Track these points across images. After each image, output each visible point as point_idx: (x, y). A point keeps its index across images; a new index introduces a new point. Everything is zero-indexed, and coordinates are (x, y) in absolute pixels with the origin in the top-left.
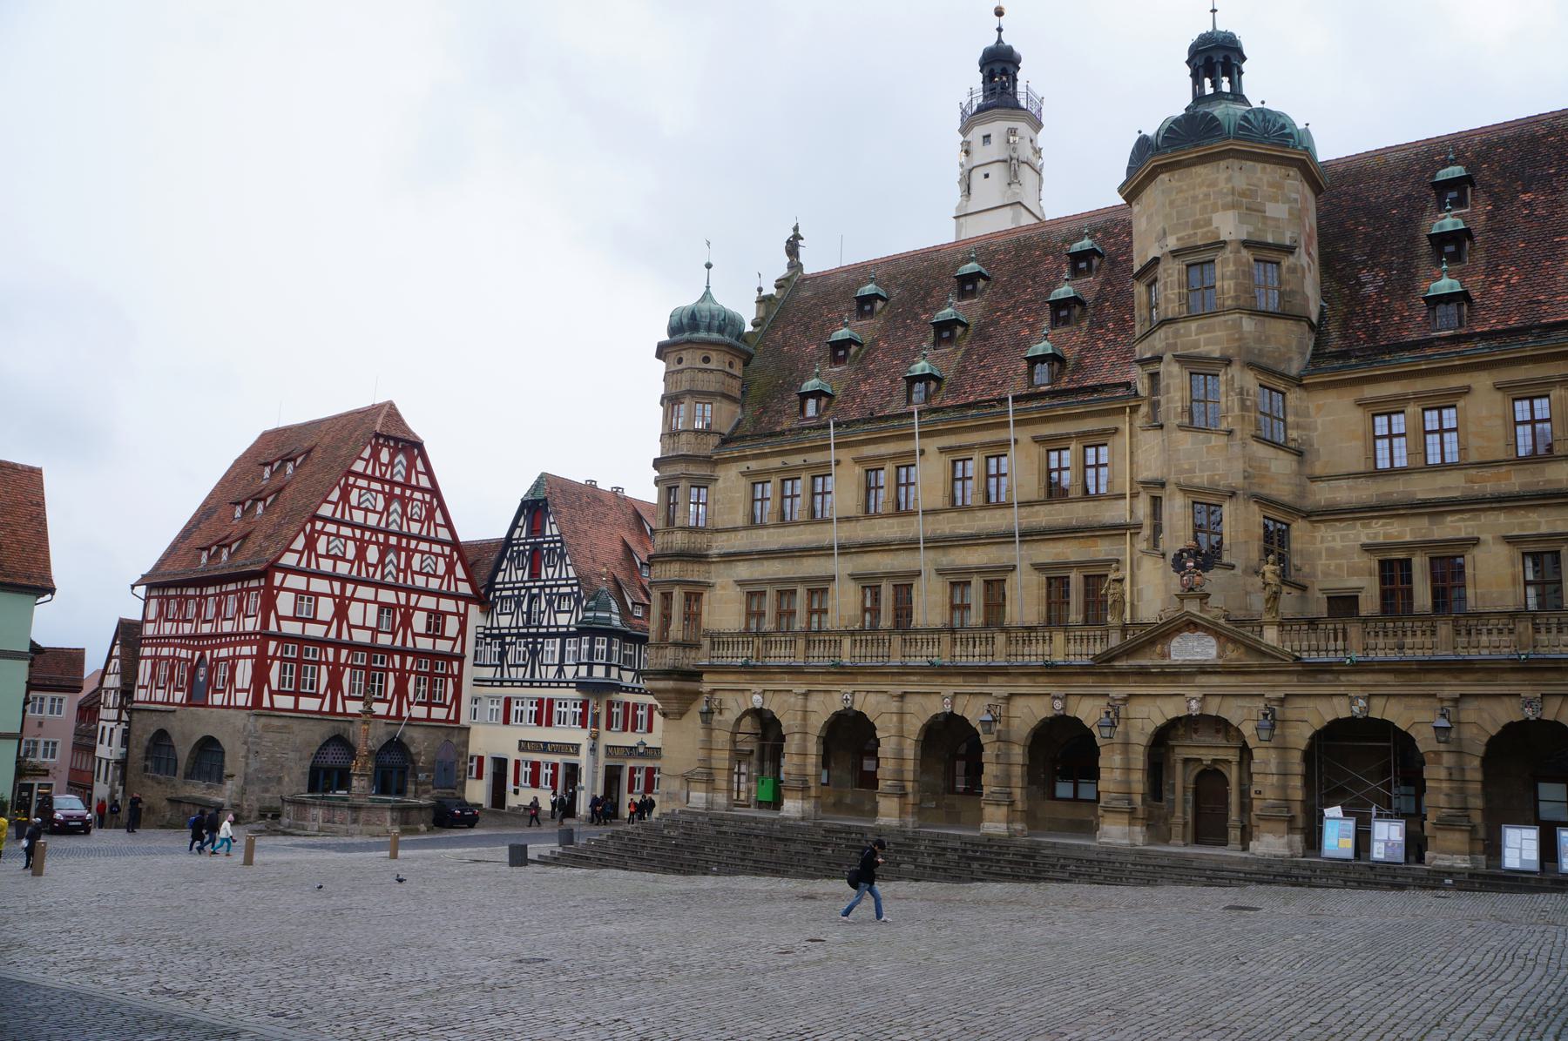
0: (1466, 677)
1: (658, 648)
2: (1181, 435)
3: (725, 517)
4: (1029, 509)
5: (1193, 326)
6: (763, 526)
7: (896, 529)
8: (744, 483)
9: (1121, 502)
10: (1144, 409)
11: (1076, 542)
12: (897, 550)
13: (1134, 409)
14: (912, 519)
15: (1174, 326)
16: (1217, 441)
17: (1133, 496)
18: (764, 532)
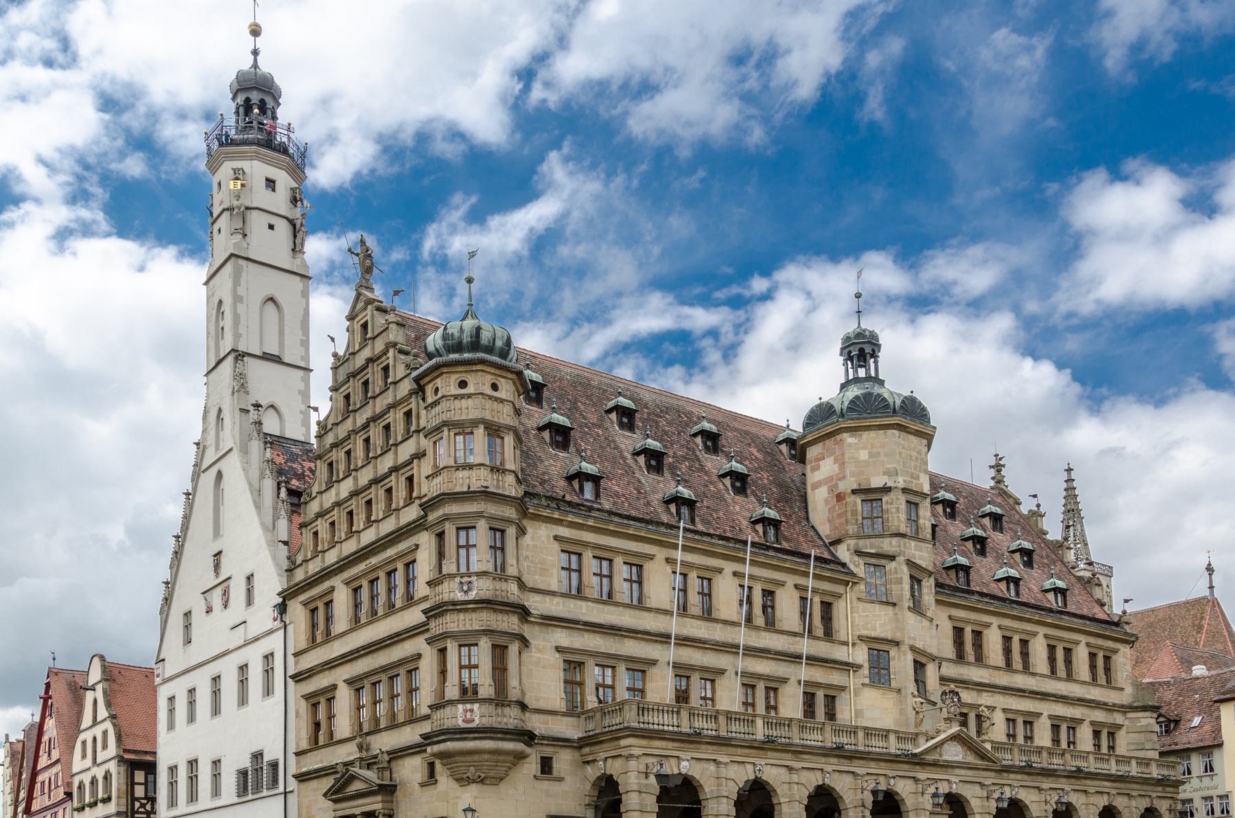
0: (1050, 779)
1: (497, 705)
2: (909, 614)
3: (537, 577)
4: (794, 638)
5: (913, 543)
6: (586, 599)
7: (703, 631)
8: (556, 546)
9: (845, 648)
10: (862, 587)
11: (821, 669)
12: (706, 648)
13: (854, 583)
14: (715, 625)
15: (903, 541)
16: (926, 623)
17: (854, 644)
18: (583, 604)
